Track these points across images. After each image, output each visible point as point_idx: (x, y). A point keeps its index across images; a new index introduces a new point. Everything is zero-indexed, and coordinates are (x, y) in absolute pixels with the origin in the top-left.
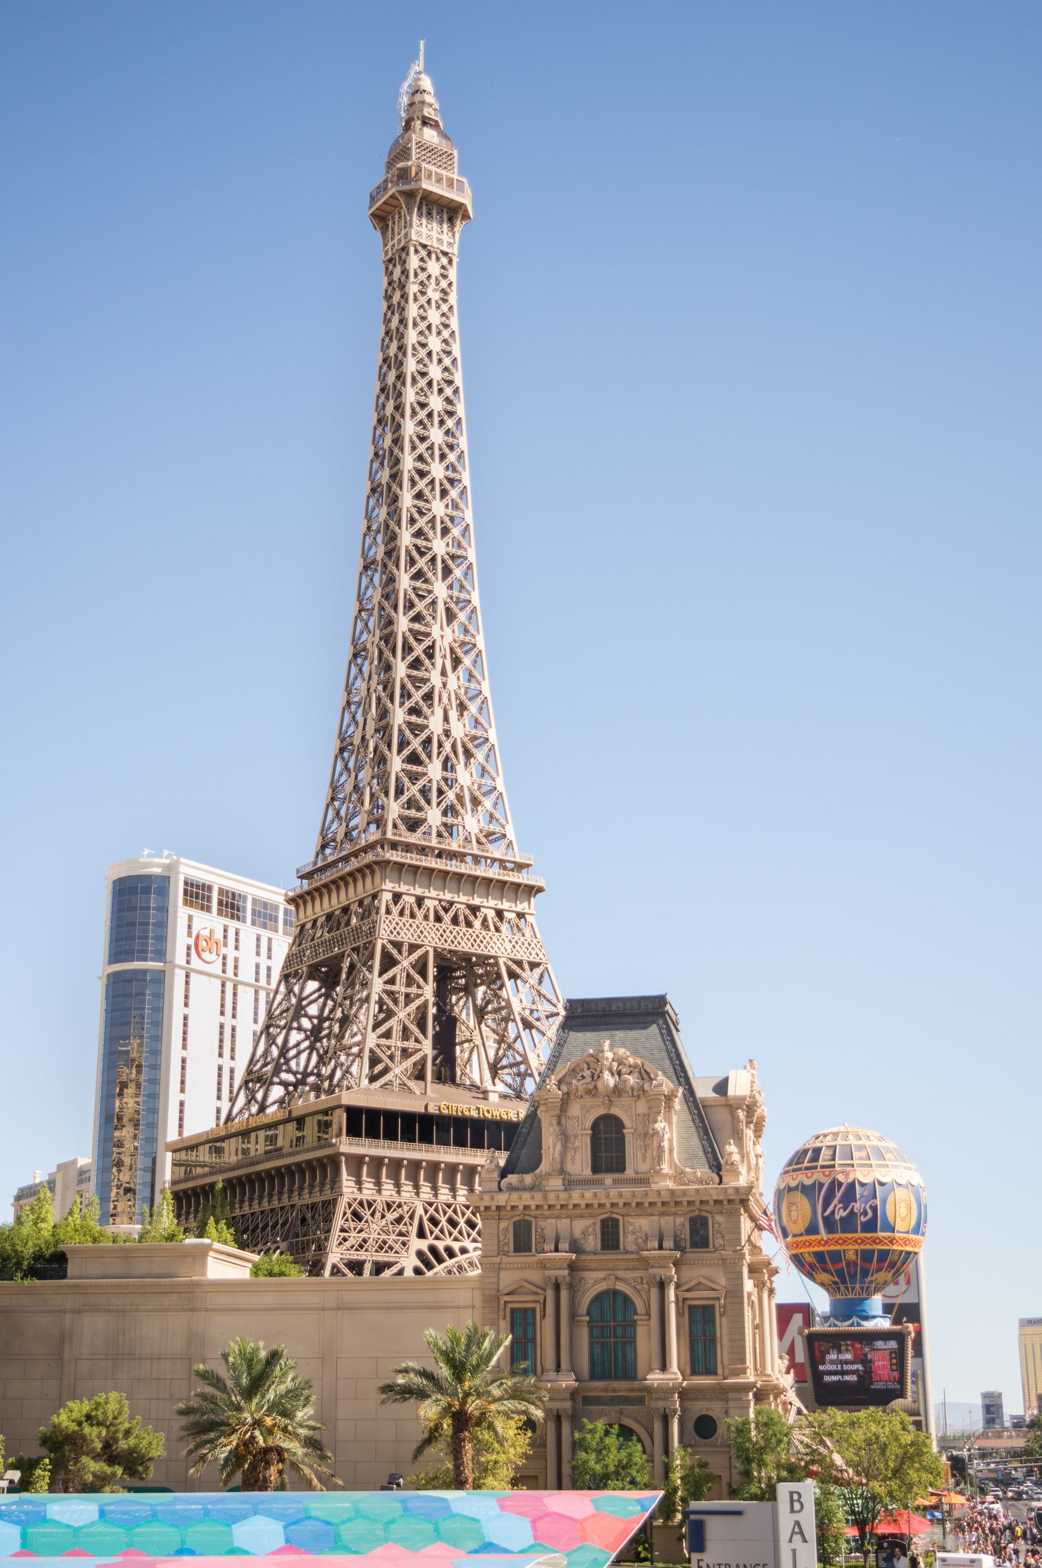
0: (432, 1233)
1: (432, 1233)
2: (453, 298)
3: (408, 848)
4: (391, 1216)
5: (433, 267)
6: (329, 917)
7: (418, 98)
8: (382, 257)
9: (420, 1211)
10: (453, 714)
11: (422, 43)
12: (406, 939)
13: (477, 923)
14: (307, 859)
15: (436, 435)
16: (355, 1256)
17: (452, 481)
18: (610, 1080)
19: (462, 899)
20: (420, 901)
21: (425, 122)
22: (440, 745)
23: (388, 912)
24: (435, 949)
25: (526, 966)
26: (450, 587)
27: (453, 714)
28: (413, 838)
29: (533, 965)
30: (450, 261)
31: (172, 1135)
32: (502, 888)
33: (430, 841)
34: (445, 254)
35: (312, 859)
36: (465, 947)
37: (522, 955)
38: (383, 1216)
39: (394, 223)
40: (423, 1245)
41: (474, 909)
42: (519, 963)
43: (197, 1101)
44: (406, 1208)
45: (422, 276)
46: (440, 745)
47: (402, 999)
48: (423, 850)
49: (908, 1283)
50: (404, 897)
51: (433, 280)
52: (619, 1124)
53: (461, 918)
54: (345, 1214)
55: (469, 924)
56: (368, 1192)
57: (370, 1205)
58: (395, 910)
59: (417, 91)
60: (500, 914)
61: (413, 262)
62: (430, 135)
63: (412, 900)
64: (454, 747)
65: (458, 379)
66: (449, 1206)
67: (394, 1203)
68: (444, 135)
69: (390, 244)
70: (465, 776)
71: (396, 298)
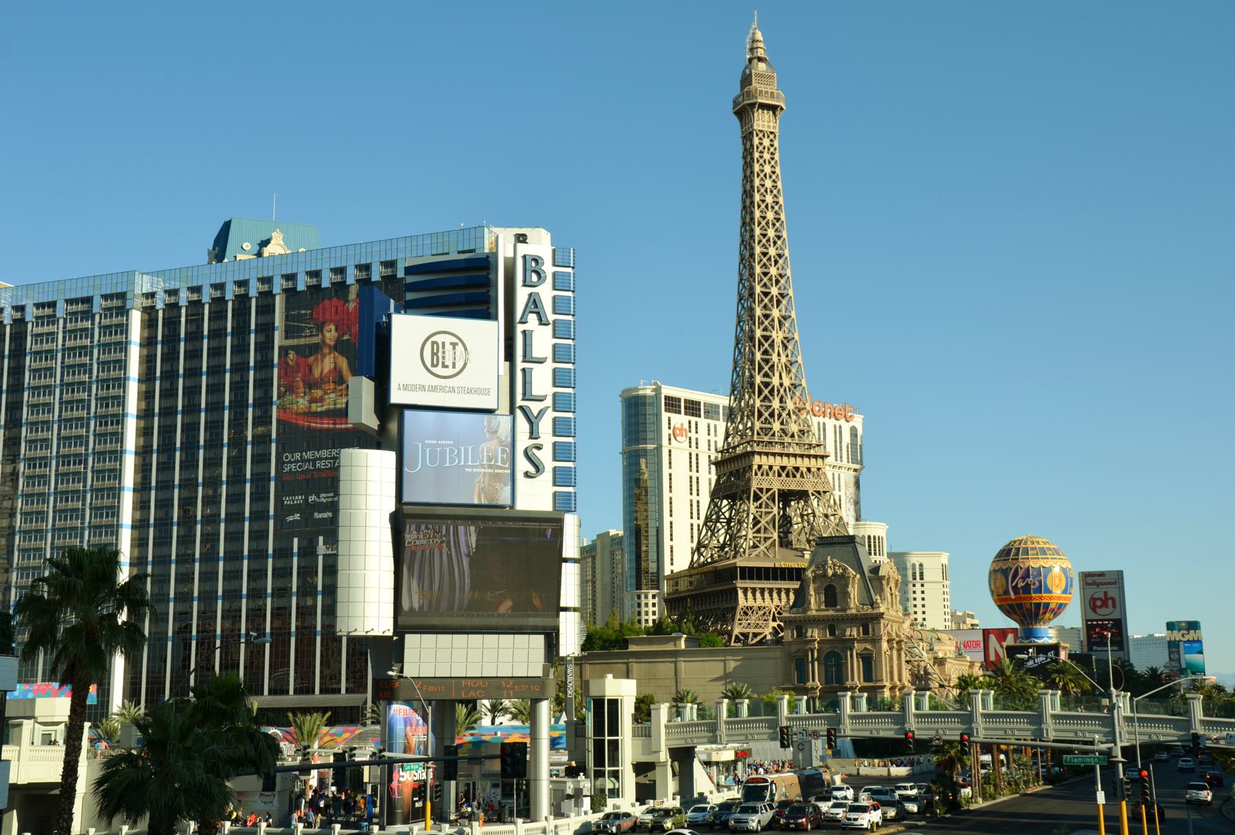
2: (777, 157)
4: (761, 613)
5: (766, 142)
7: (755, 45)
8: (740, 134)
10: (784, 375)
13: (798, 475)
16: (746, 631)
17: (780, 256)
18: (830, 572)
19: (790, 463)
20: (771, 467)
21: (760, 59)
28: (766, 439)
31: (667, 572)
36: (793, 487)
40: (775, 624)
41: (797, 469)
42: (818, 492)
43: (679, 554)
45: (761, 148)
49: (1114, 606)
52: (834, 588)
55: (794, 476)
56: (751, 602)
59: (754, 41)
60: (809, 470)
62: (762, 66)
65: (781, 200)
68: (769, 65)
70: (790, 405)
71: (748, 159)
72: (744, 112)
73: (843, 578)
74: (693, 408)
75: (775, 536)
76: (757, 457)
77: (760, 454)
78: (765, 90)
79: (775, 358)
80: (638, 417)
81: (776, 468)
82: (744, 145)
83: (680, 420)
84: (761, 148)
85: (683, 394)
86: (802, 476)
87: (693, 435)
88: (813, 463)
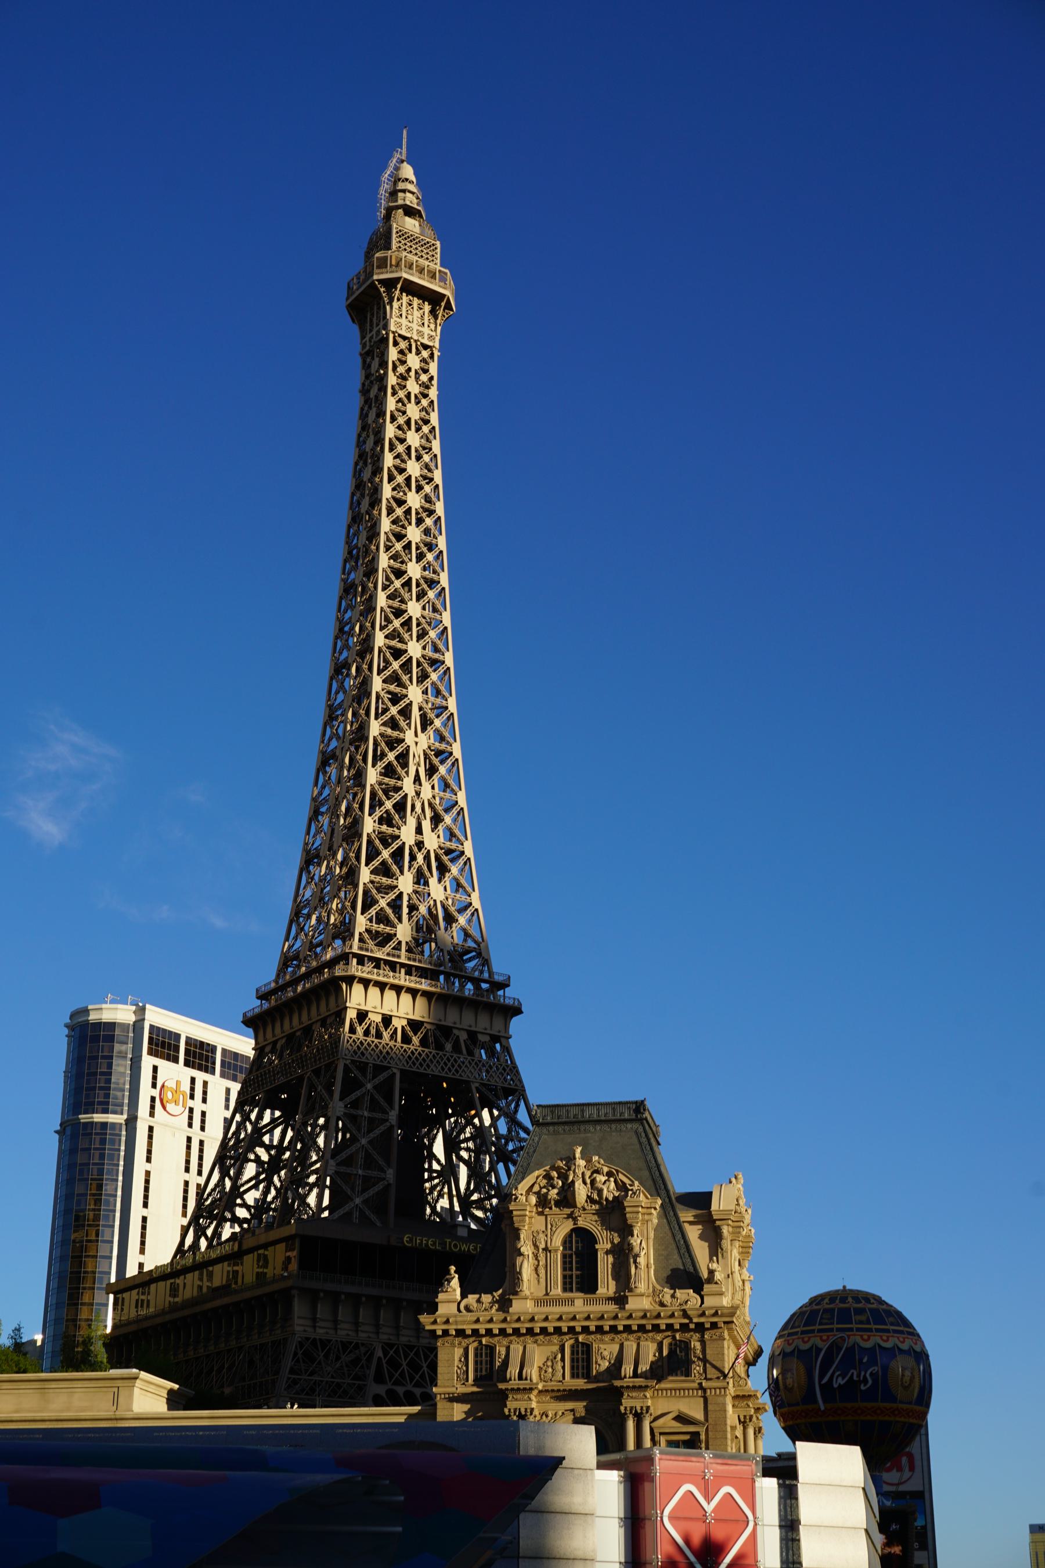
0: (391, 1376)
1: (391, 1376)
2: (433, 393)
3: (377, 963)
5: (413, 361)
6: (290, 1037)
7: (401, 186)
9: (380, 1353)
10: (426, 825)
11: (405, 132)
12: (371, 1061)
13: (448, 1047)
14: (267, 975)
15: (414, 534)
20: (387, 1020)
21: (409, 212)
22: (413, 858)
23: (353, 1030)
24: (402, 1071)
25: (500, 1093)
26: (425, 692)
27: (426, 825)
29: (508, 1092)
30: (432, 356)
32: (475, 1004)
33: (399, 957)
34: (426, 347)
35: (273, 977)
37: (497, 1081)
38: (338, 1358)
39: (372, 315)
44: (363, 1349)
46: (413, 858)
47: (365, 1124)
48: (393, 966)
50: (370, 1015)
51: (412, 374)
53: (431, 1040)
54: (296, 1354)
57: (324, 1343)
58: (360, 1030)
60: (472, 1035)
61: (393, 354)
62: (411, 224)
63: (378, 1019)
64: (427, 857)
66: (411, 1348)
67: (351, 1343)
69: (369, 336)
70: (437, 890)
72: (367, 306)
73: (614, 1214)
74: (200, 1056)
75: (390, 1174)
76: (358, 989)
77: (366, 983)
78: (417, 252)
79: (408, 785)
80: (93, 1061)
81: (398, 1023)
82: (366, 366)
83: (175, 1074)
84: (401, 369)
85: (187, 1028)
86: (456, 1048)
87: (197, 1105)
88: (482, 1023)
